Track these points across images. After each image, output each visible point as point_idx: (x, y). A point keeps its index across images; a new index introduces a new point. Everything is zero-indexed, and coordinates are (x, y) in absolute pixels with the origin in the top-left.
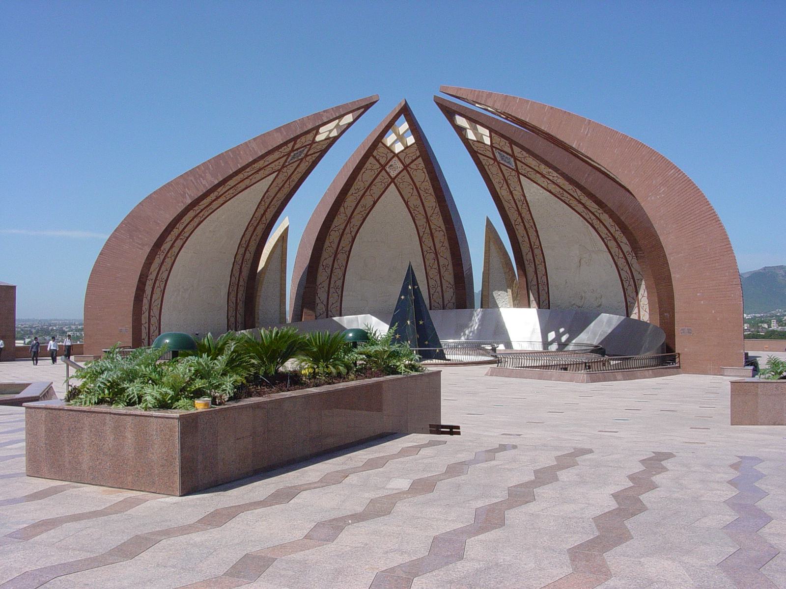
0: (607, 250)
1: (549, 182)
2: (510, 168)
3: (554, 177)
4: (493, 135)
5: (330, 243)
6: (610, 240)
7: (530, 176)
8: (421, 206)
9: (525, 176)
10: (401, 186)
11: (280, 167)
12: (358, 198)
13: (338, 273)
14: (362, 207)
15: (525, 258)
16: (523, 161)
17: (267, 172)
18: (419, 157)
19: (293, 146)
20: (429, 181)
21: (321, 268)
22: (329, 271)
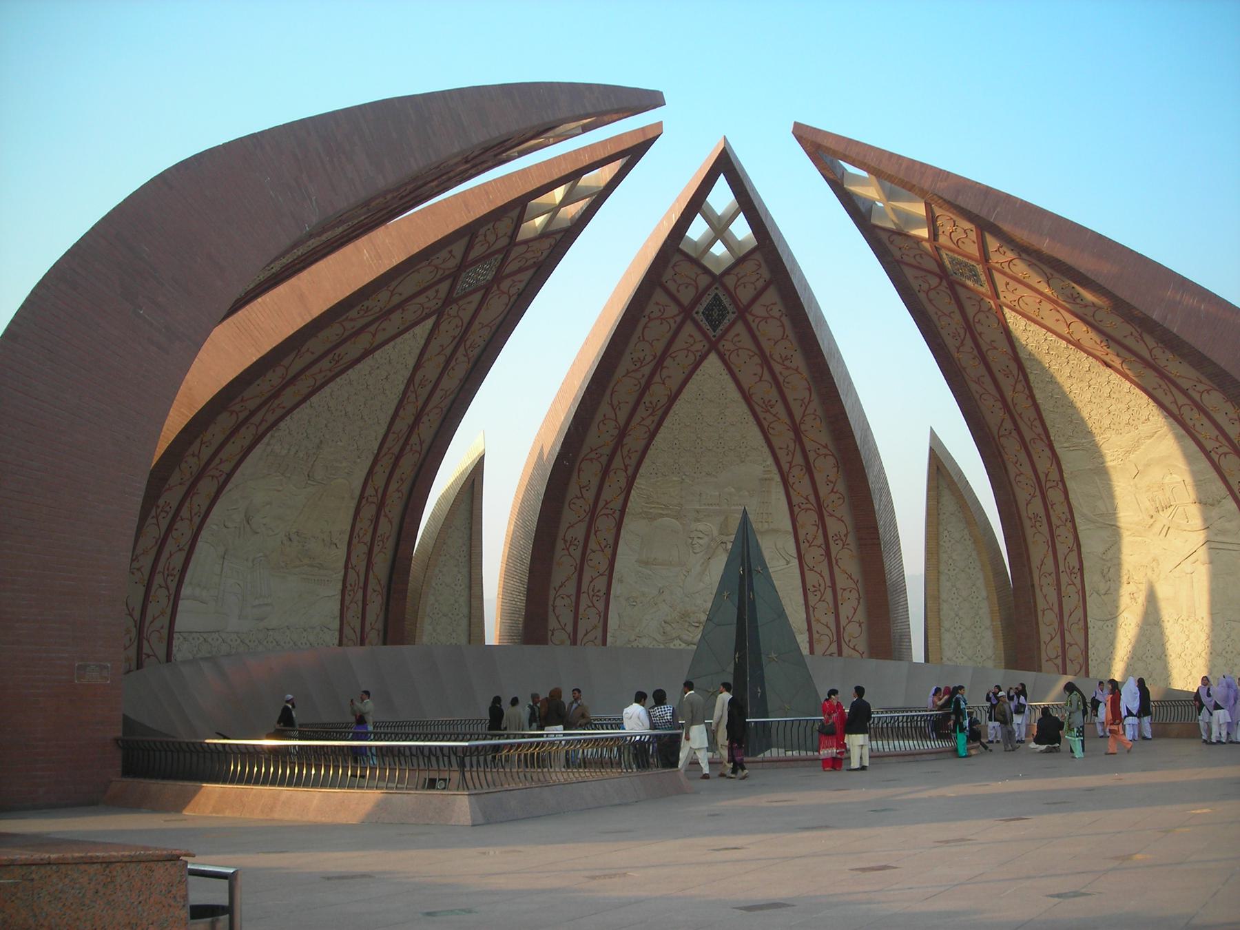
0: (790, 528)
1: (767, 376)
3: (788, 368)
4: (758, 256)
6: (807, 510)
7: (733, 358)
9: (721, 356)
12: (347, 334)
13: (184, 528)
15: (561, 535)
16: (754, 326)
20: (494, 328)
21: (153, 513)
22: (164, 527)
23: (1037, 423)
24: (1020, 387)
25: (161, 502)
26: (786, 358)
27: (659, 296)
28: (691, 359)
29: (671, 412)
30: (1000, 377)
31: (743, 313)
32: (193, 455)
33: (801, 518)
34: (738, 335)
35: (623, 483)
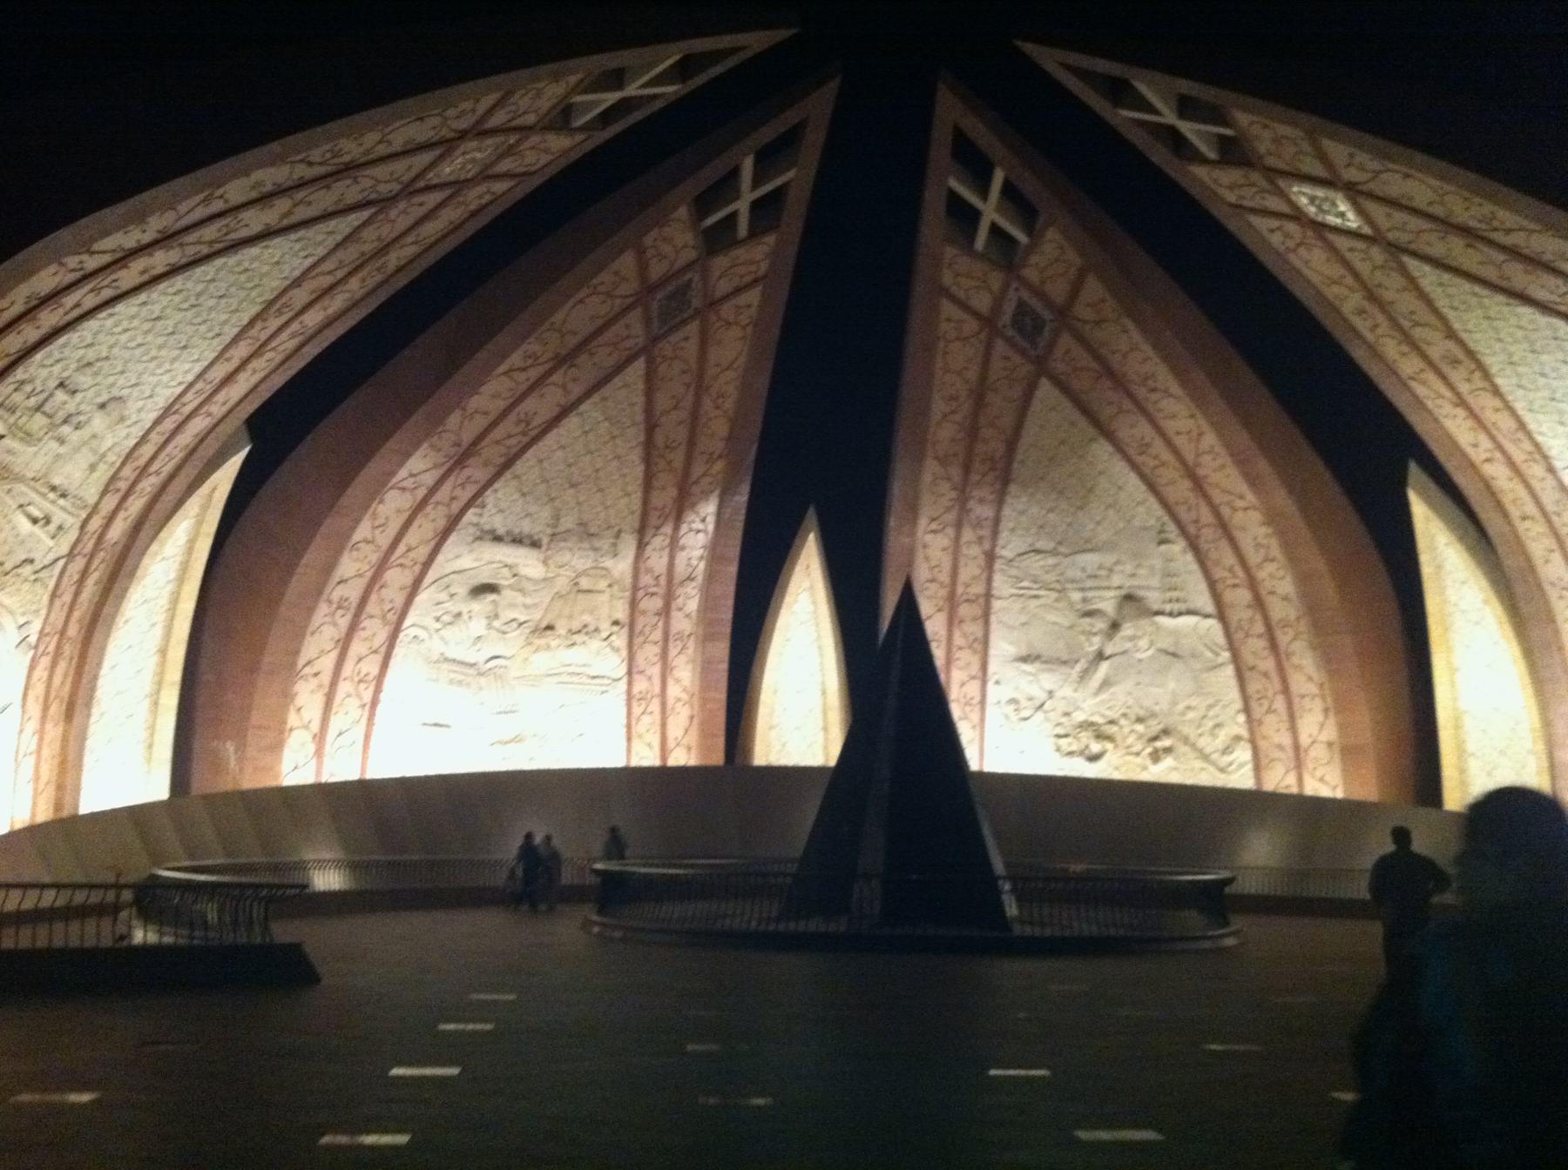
1: (1127, 404)
2: (1023, 353)
5: (374, 528)
6: (1235, 586)
7: (1076, 385)
8: (683, 448)
10: (663, 369)
11: (396, 187)
12: (524, 387)
13: (374, 630)
14: (519, 422)
17: (353, 196)
18: (756, 281)
19: (490, 111)
21: (323, 609)
22: (344, 622)
23: (1520, 435)
24: (1477, 374)
25: (336, 595)
26: (1146, 379)
27: (948, 308)
28: (1017, 392)
29: (1015, 465)
30: (1446, 369)
31: (1063, 313)
32: (367, 542)
33: (1229, 596)
34: (1068, 352)
35: (981, 561)
